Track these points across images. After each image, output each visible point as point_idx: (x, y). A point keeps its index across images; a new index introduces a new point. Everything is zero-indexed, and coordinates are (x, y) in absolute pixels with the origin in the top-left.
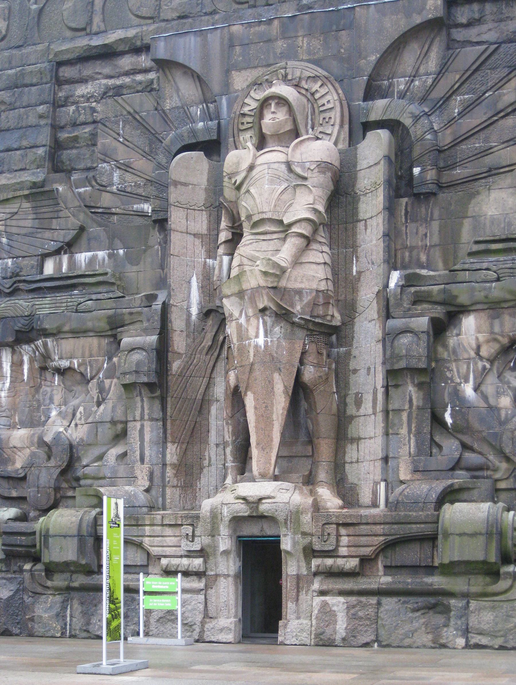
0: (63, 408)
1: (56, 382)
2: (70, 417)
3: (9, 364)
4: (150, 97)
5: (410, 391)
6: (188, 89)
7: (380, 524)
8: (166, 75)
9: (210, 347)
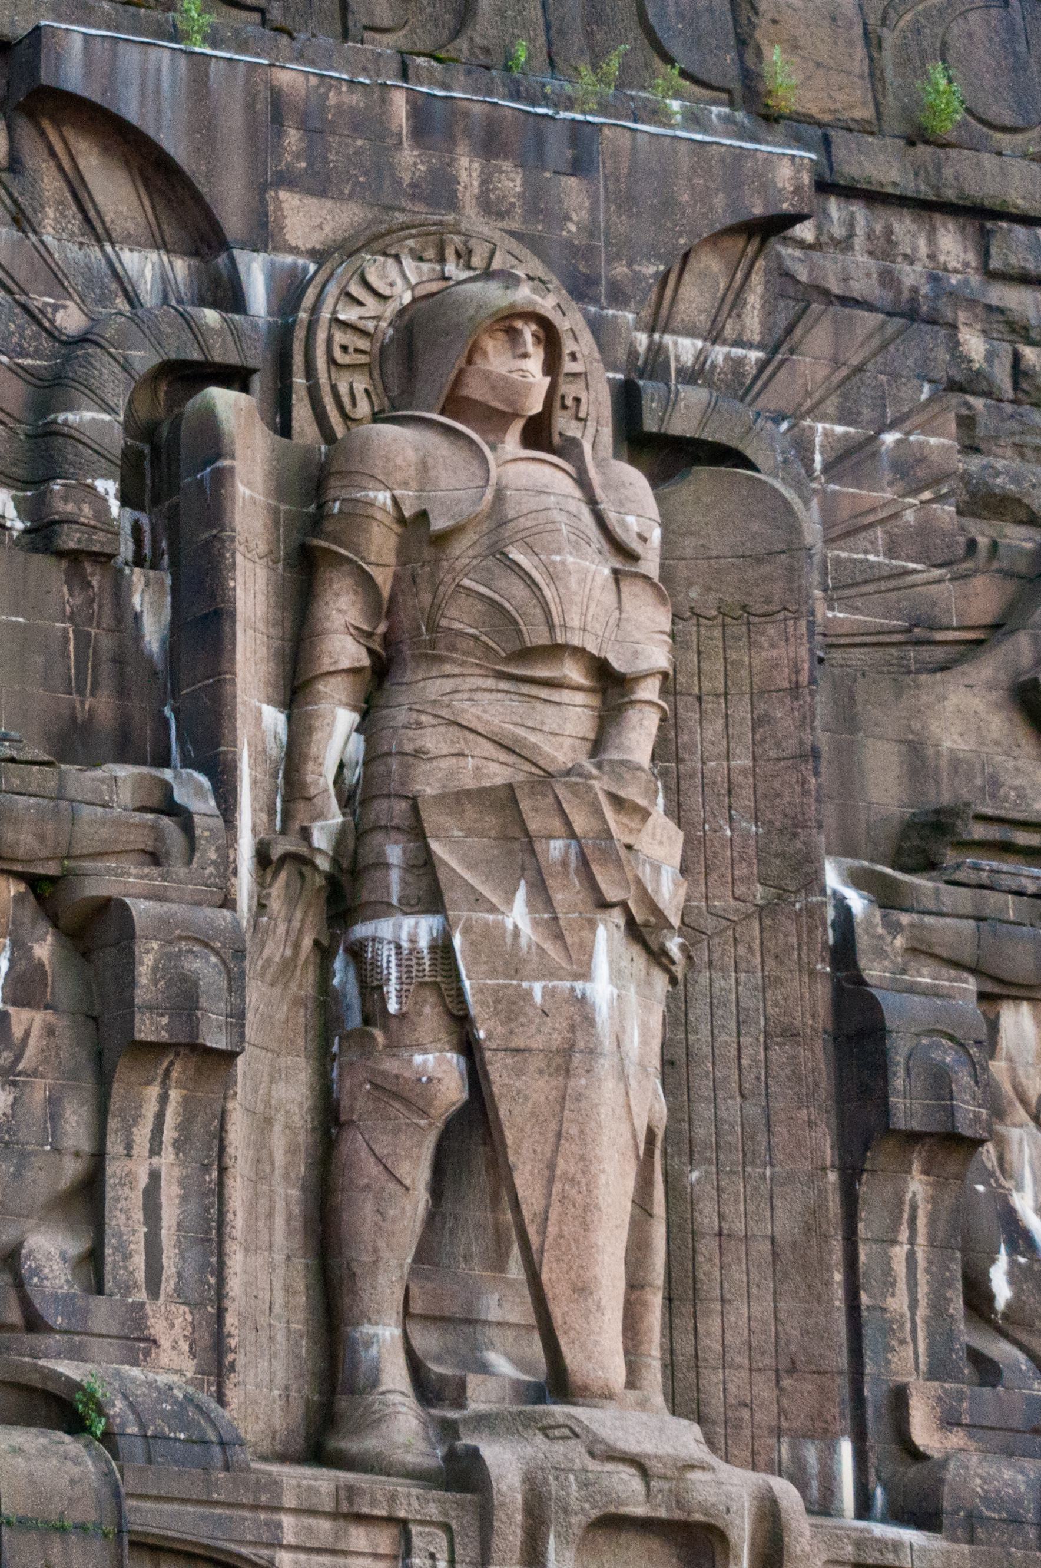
5: (914, 1194)
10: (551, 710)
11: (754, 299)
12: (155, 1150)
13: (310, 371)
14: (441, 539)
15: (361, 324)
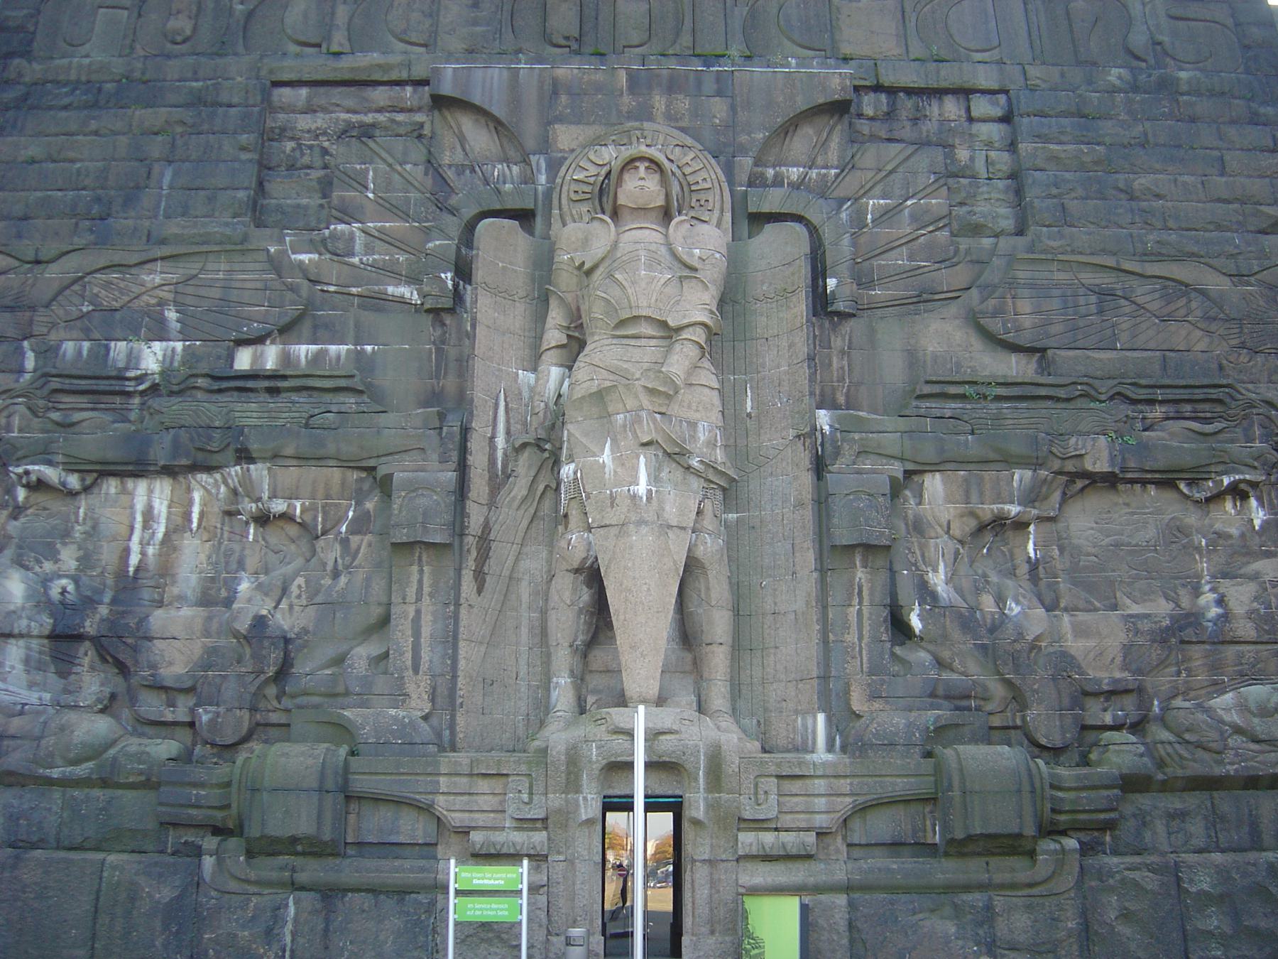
0: (262, 578)
1: (251, 538)
2: (278, 592)
3: (166, 503)
4: (420, 145)
6: (480, 139)
7: (846, 777)
8: (445, 118)
10: (639, 350)
11: (834, 143)
13: (560, 209)
14: (589, 273)
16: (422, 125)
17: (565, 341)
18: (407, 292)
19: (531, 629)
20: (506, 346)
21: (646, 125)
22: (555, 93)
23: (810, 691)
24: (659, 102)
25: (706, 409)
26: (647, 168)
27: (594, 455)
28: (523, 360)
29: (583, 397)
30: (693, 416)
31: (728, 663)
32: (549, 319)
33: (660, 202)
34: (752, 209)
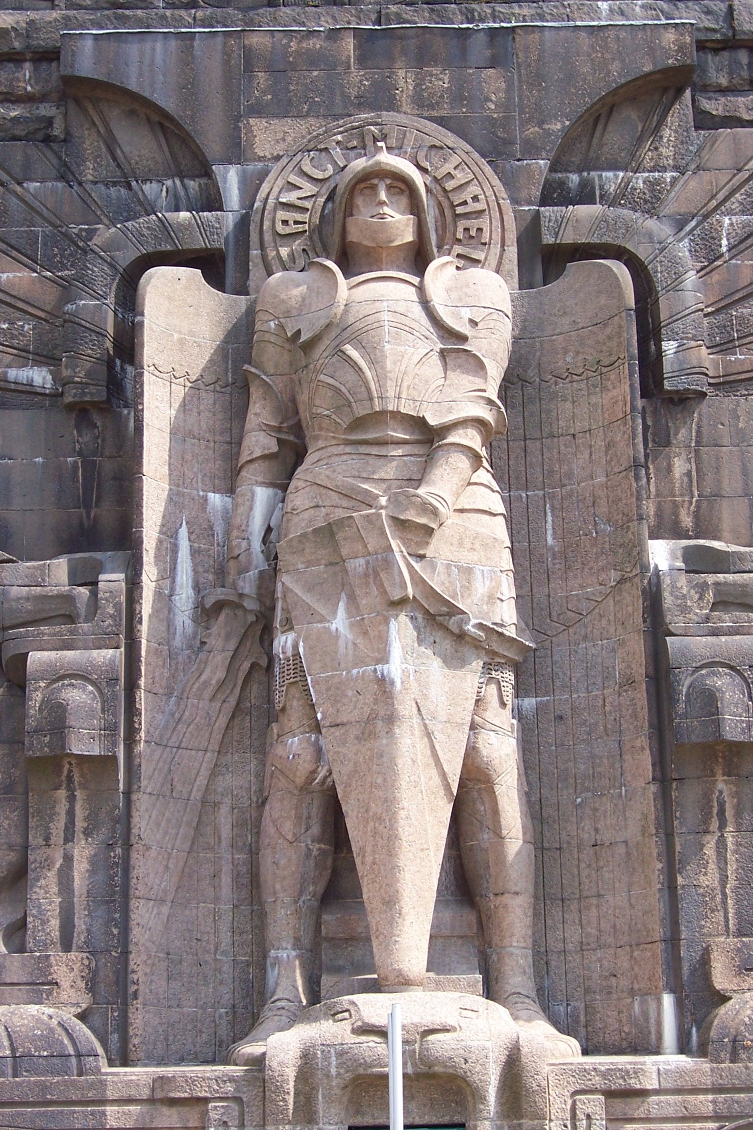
4: (49, 153)
7: (705, 1091)
9: (222, 684)
12: (69, 837)
13: (262, 247)
14: (309, 346)
15: (299, 203)
16: (50, 122)
17: (275, 448)
18: (39, 377)
19: (236, 877)
20: (188, 457)
21: (387, 116)
22: (249, 68)
23: (654, 957)
24: (404, 80)
25: (485, 546)
26: (389, 188)
27: (323, 620)
28: (213, 477)
29: (304, 535)
30: (465, 557)
31: (528, 921)
32: (250, 416)
33: (409, 237)
34: (548, 239)
